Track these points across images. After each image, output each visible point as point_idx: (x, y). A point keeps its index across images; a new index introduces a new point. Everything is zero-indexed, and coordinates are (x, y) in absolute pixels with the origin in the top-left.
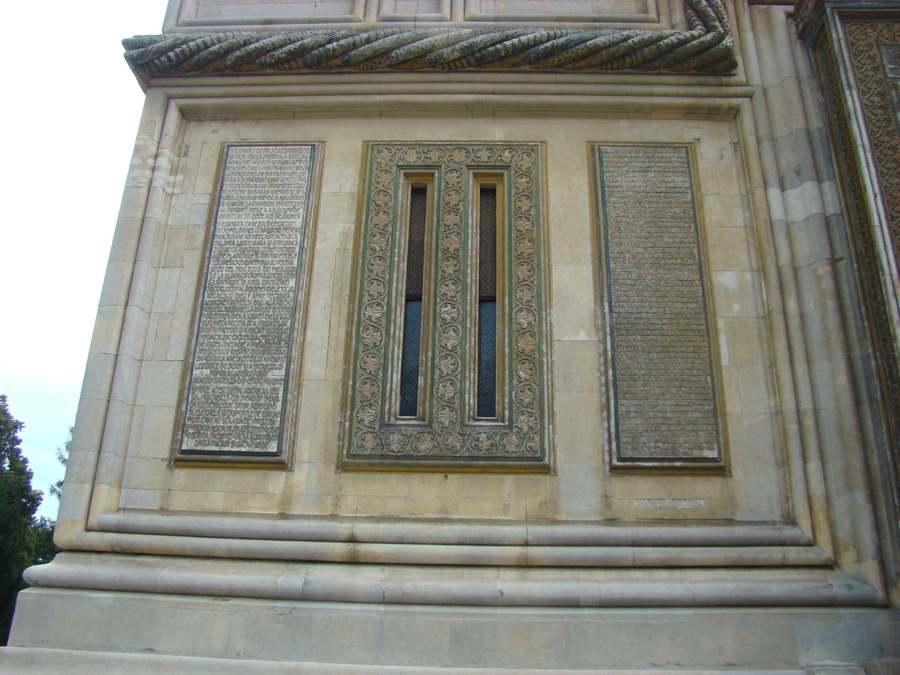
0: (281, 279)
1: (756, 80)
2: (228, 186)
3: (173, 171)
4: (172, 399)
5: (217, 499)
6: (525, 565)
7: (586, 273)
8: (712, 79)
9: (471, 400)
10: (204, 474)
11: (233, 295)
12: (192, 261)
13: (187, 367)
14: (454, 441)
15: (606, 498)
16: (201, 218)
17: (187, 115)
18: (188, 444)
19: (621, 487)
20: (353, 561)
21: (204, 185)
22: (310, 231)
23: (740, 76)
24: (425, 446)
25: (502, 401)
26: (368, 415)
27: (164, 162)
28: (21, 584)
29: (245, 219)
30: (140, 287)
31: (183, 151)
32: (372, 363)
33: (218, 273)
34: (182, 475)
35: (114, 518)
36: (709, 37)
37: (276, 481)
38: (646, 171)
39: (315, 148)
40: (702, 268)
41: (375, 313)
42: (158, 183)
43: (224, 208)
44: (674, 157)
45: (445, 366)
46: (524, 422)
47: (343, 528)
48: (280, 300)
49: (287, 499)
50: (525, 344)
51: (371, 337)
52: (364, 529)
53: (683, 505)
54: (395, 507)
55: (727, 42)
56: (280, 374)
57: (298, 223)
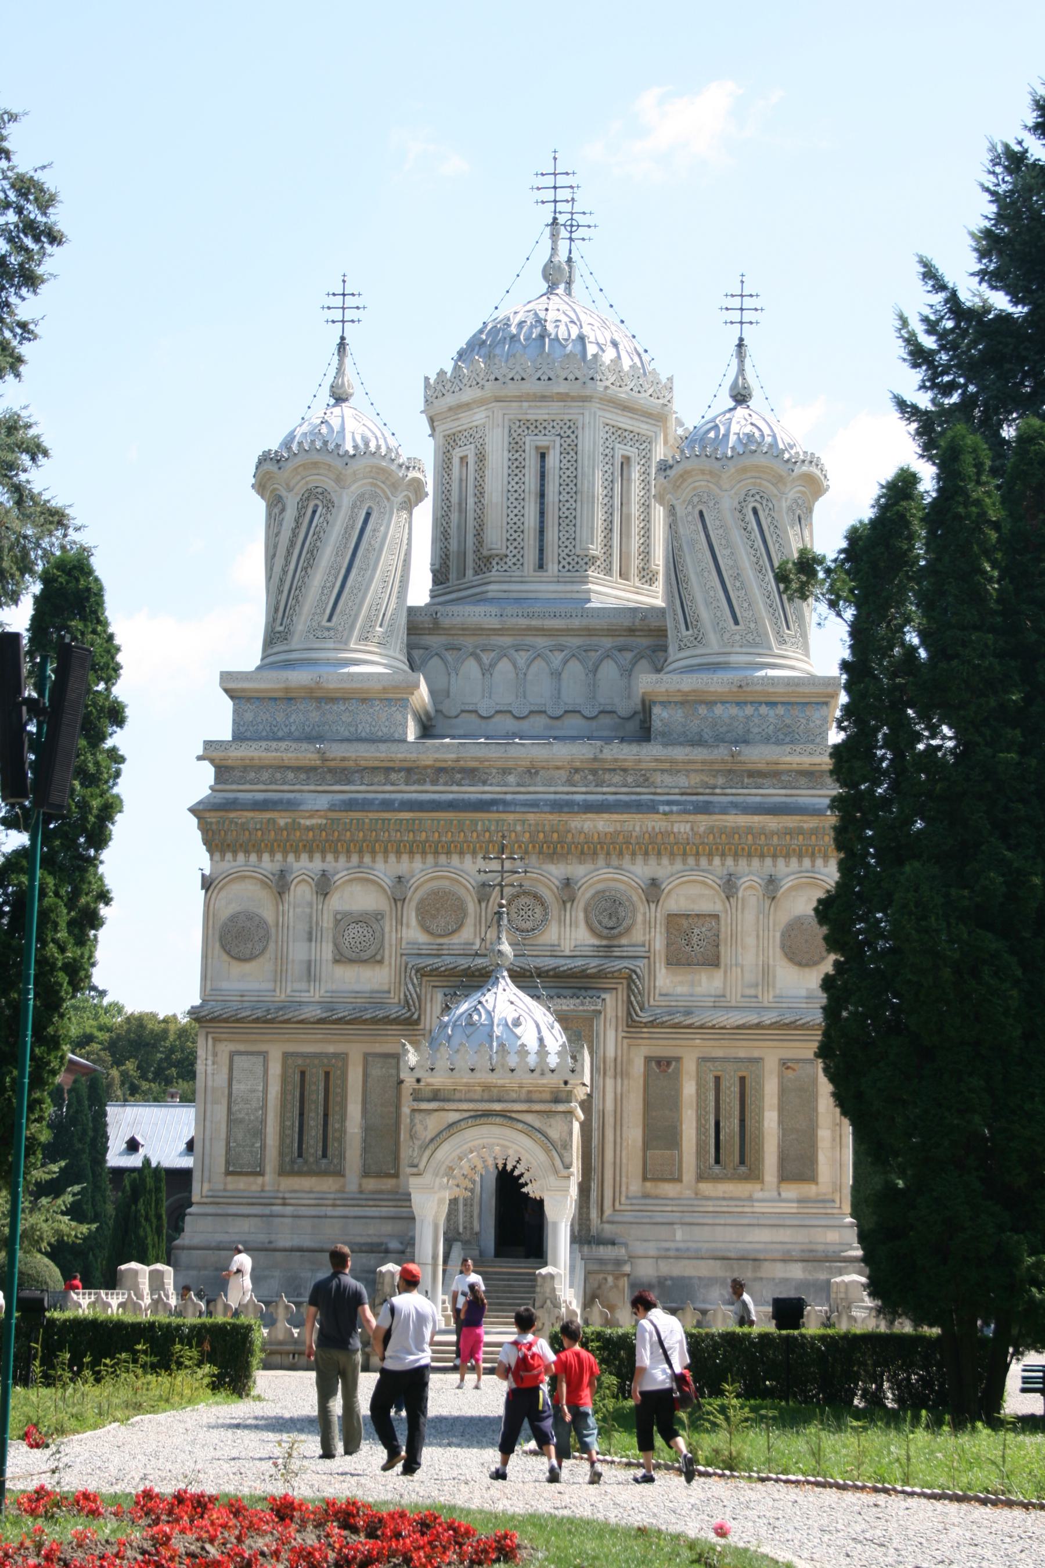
0: (256, 1110)
1: (428, 1027)
2: (235, 1073)
3: (213, 1063)
4: (224, 1153)
5: (242, 1186)
6: (334, 1205)
7: (359, 1107)
8: (410, 1027)
9: (320, 1153)
10: (236, 1178)
11: (240, 1116)
12: (225, 1102)
13: (228, 1143)
14: (314, 1167)
15: (360, 1185)
16: (226, 1084)
17: (215, 1040)
18: (231, 1169)
19: (365, 1181)
20: (284, 1204)
21: (225, 1070)
22: (265, 1091)
23: (421, 1027)
24: (305, 1169)
25: (330, 1152)
26: (287, 1159)
27: (209, 1062)
28: (185, 1215)
29: (242, 1087)
30: (208, 1114)
31: (215, 1055)
32: (288, 1141)
33: (235, 1108)
34: (230, 1178)
35: (210, 1194)
36: (408, 1014)
37: (260, 1179)
38: (382, 1068)
39: (265, 1055)
40: (398, 1107)
41: (288, 1123)
42: (209, 1071)
43: (234, 1082)
44: (394, 1061)
45: (312, 1142)
46: (335, 1161)
47: (280, 1195)
48: (257, 1118)
49: (263, 1185)
50: (337, 1135)
51: (288, 1132)
52: (287, 1195)
53: (383, 1187)
54: (296, 1187)
55: (415, 1016)
56: (258, 1145)
57: (261, 1088)
